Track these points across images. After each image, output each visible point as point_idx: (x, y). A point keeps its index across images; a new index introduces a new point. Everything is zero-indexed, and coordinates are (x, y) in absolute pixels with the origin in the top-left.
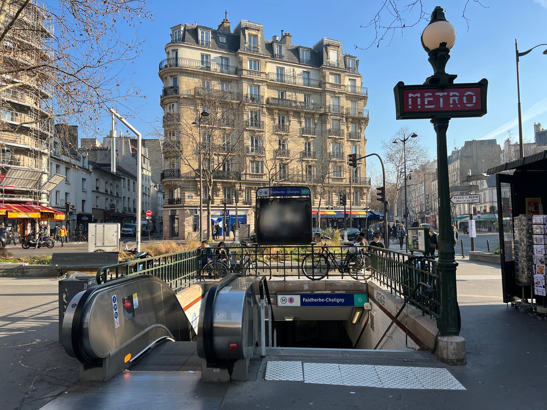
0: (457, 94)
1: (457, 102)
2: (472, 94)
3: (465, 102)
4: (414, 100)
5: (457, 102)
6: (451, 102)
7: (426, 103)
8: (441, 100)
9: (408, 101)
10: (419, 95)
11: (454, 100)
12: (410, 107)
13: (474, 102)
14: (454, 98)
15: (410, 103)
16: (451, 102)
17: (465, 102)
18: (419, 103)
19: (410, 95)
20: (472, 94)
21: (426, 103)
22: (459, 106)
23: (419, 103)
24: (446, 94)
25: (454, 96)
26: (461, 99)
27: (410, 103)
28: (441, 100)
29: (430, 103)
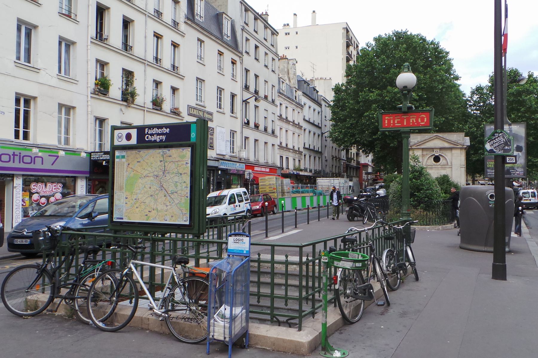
0: (415, 117)
1: (415, 122)
2: (424, 116)
3: (420, 121)
4: (389, 121)
5: (415, 122)
6: (411, 121)
7: (396, 122)
8: (405, 120)
9: (385, 121)
10: (392, 118)
11: (413, 120)
12: (386, 125)
13: (425, 121)
14: (413, 119)
15: (386, 122)
16: (411, 121)
17: (420, 121)
18: (392, 122)
19: (386, 118)
20: (424, 116)
21: (396, 122)
22: (416, 124)
23: (392, 122)
24: (408, 116)
25: (413, 118)
26: (417, 120)
27: (386, 122)
28: (405, 120)
29: (398, 122)
